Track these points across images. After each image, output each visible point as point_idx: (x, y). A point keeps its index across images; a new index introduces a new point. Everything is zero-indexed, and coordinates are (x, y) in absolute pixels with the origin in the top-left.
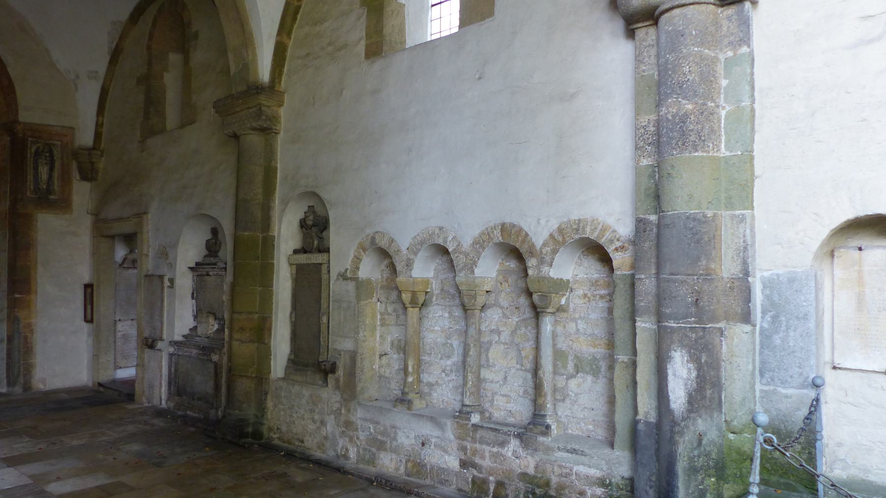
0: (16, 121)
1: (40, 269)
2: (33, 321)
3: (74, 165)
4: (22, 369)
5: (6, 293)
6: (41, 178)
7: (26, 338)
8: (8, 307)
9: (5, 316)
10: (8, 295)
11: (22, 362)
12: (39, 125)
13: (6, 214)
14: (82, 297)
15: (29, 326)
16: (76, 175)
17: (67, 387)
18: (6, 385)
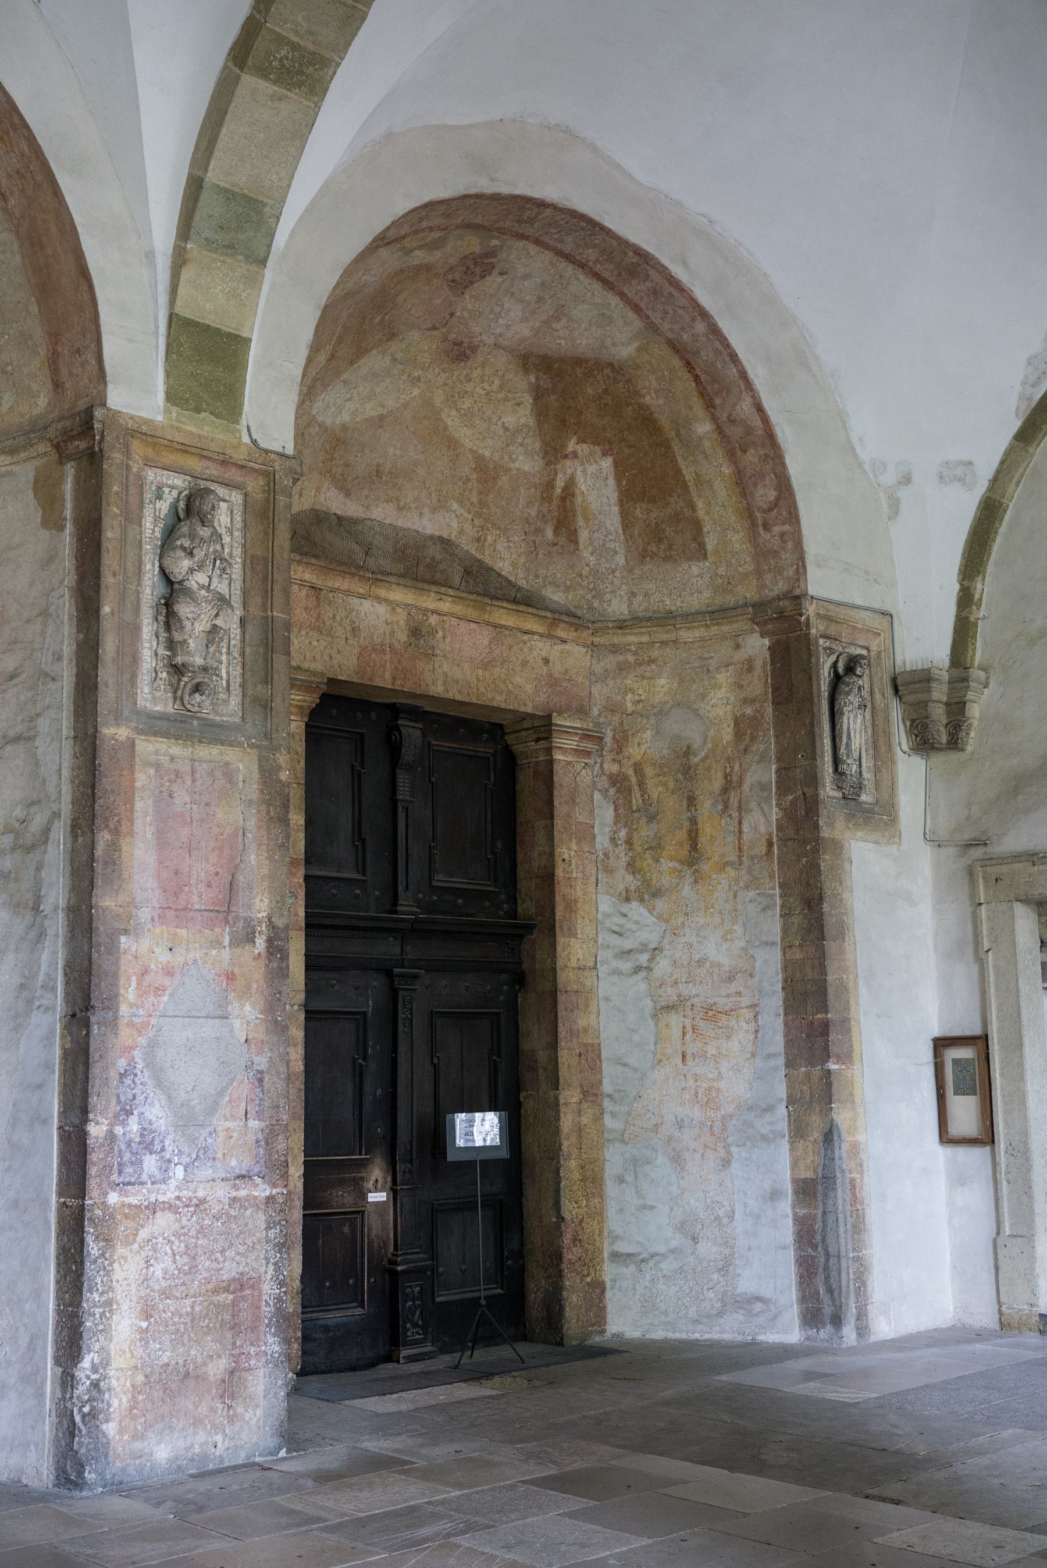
0: (797, 598)
1: (863, 990)
2: (861, 1137)
3: (896, 711)
4: (852, 1277)
5: (781, 1061)
6: (848, 745)
7: (852, 1181)
8: (791, 1100)
9: (783, 1125)
10: (790, 1064)
11: (851, 1255)
12: (839, 604)
13: (770, 844)
14: (929, 1072)
15: (855, 1149)
16: (901, 738)
17: (922, 1329)
18: (797, 1322)
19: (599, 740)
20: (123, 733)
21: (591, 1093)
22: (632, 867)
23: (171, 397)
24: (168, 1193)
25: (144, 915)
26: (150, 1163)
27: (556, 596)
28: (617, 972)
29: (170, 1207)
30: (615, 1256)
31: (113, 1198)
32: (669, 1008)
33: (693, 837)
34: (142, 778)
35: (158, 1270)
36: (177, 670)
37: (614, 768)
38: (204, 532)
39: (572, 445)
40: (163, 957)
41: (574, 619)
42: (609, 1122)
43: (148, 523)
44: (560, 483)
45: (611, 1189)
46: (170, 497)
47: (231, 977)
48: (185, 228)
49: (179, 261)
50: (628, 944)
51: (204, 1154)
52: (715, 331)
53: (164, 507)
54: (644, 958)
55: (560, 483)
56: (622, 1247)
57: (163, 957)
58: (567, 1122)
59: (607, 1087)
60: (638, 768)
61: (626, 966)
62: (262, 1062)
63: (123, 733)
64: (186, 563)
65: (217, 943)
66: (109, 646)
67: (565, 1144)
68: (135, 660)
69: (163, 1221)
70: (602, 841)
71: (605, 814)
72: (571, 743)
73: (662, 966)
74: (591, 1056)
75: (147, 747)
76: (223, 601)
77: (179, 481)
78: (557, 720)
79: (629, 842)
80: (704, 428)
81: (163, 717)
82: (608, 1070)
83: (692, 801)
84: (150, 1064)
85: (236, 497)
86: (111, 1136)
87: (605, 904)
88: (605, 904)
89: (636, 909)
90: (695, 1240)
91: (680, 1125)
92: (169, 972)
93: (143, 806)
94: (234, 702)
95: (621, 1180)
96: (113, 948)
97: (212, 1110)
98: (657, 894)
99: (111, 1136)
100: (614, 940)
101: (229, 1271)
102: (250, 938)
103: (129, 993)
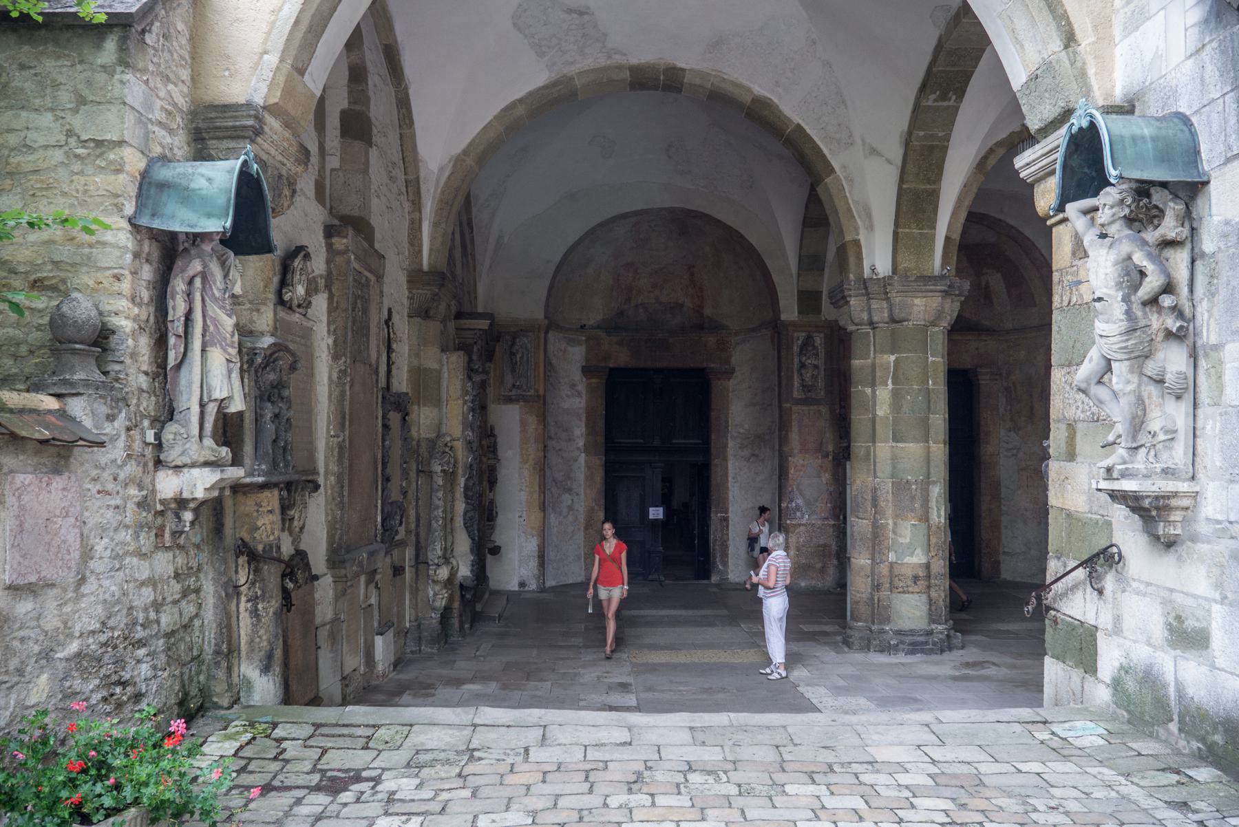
19: (1001, 375)
20: (788, 405)
21: (996, 497)
22: (1012, 420)
23: (799, 313)
24: (804, 521)
25: (796, 451)
26: (798, 514)
27: (987, 323)
28: (1006, 456)
29: (803, 525)
30: (1004, 553)
31: (788, 522)
32: (1023, 469)
33: (1032, 408)
34: (794, 417)
35: (801, 540)
36: (804, 386)
37: (1005, 384)
38: (810, 348)
39: (985, 270)
40: (802, 462)
41: (991, 332)
42: (1004, 508)
43: (795, 348)
44: (984, 283)
45: (1003, 531)
46: (801, 339)
47: (821, 467)
48: (799, 268)
49: (799, 276)
50: (1010, 446)
51: (814, 512)
52: (1019, 232)
53: (800, 342)
54: (1015, 451)
55: (984, 283)
56: (1006, 550)
57: (802, 462)
58: (984, 507)
59: (1003, 495)
60: (1014, 383)
61: (1010, 454)
62: (831, 489)
63: (788, 405)
64: (804, 358)
65: (817, 458)
66: (784, 382)
67: (983, 515)
68: (793, 386)
69: (802, 528)
70: (1001, 410)
71: (1003, 401)
72: (988, 377)
73: (1021, 454)
74: (997, 485)
75: (795, 408)
76: (816, 367)
77: (804, 334)
78: (979, 370)
79: (1011, 410)
80: (1027, 262)
81: (801, 399)
82: (1003, 490)
83: (1031, 396)
84: (798, 489)
85: (822, 335)
86: (787, 507)
87: (1003, 432)
88: (1003, 432)
89: (1013, 435)
90: (1030, 549)
91: (1026, 510)
92: (803, 466)
93: (795, 425)
94: (823, 393)
95: (1006, 527)
96: (787, 460)
97: (817, 501)
98: (1019, 429)
99: (787, 507)
100: (1005, 445)
101: (822, 542)
102: (827, 456)
103: (792, 471)
